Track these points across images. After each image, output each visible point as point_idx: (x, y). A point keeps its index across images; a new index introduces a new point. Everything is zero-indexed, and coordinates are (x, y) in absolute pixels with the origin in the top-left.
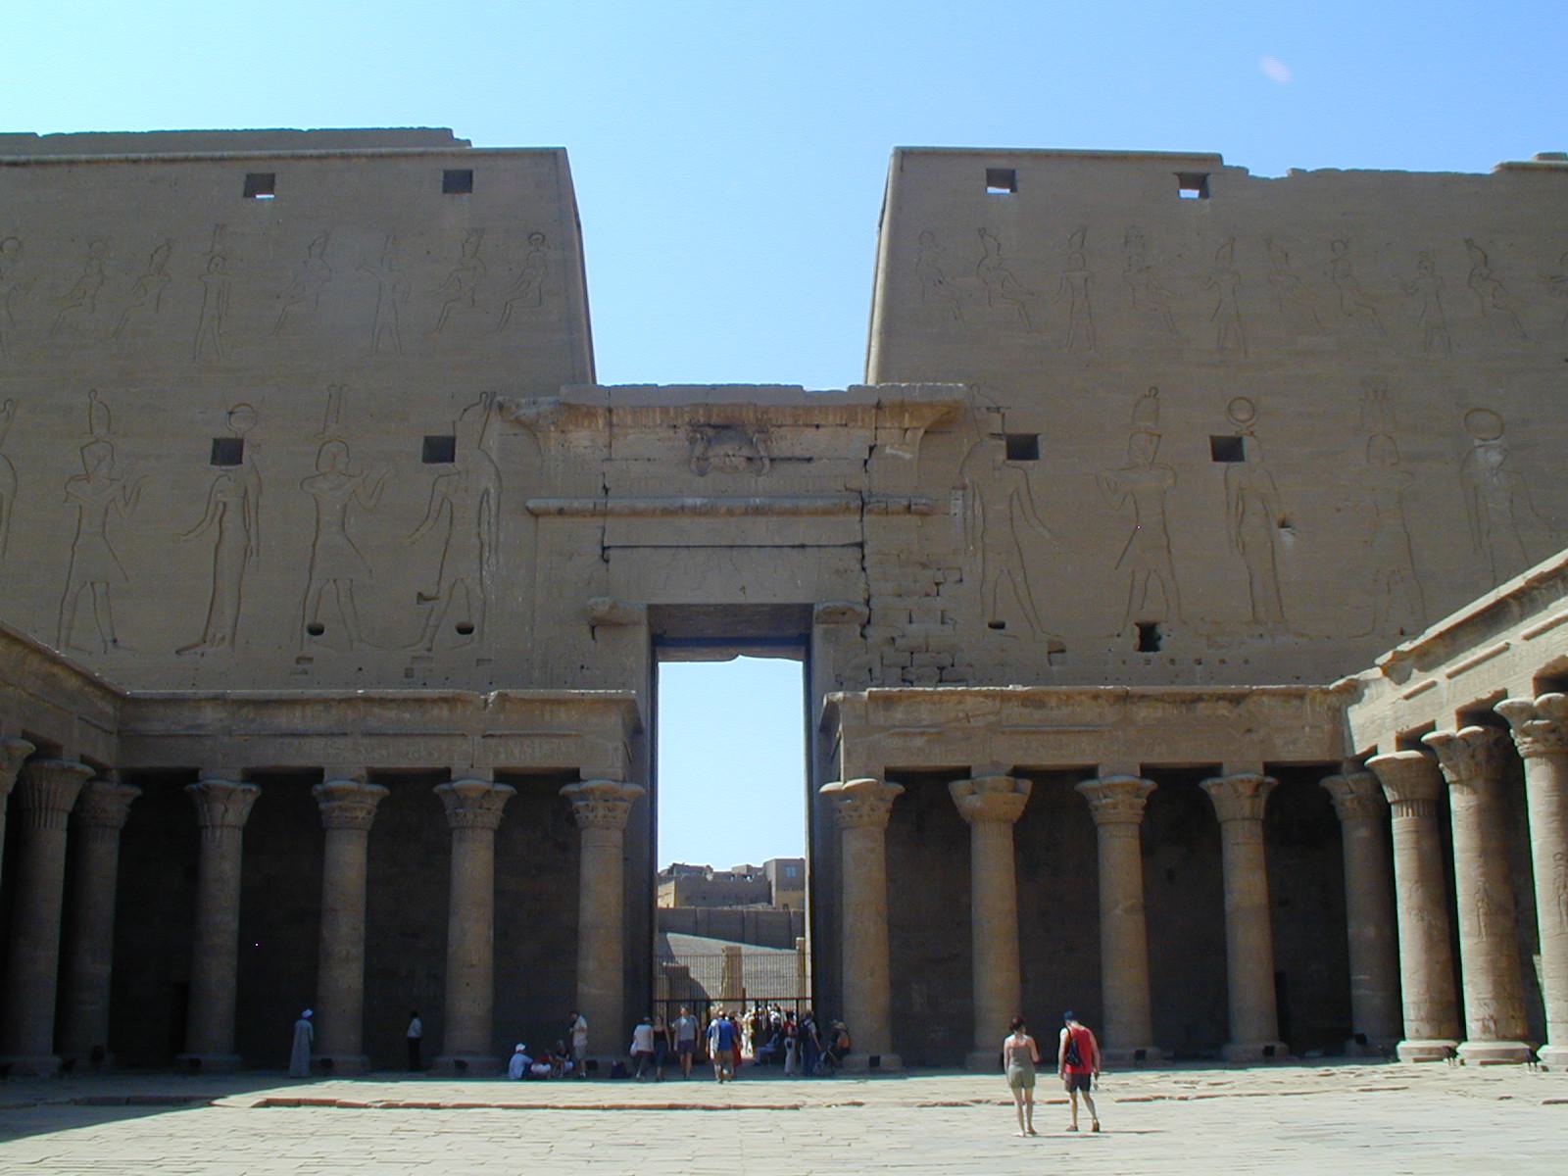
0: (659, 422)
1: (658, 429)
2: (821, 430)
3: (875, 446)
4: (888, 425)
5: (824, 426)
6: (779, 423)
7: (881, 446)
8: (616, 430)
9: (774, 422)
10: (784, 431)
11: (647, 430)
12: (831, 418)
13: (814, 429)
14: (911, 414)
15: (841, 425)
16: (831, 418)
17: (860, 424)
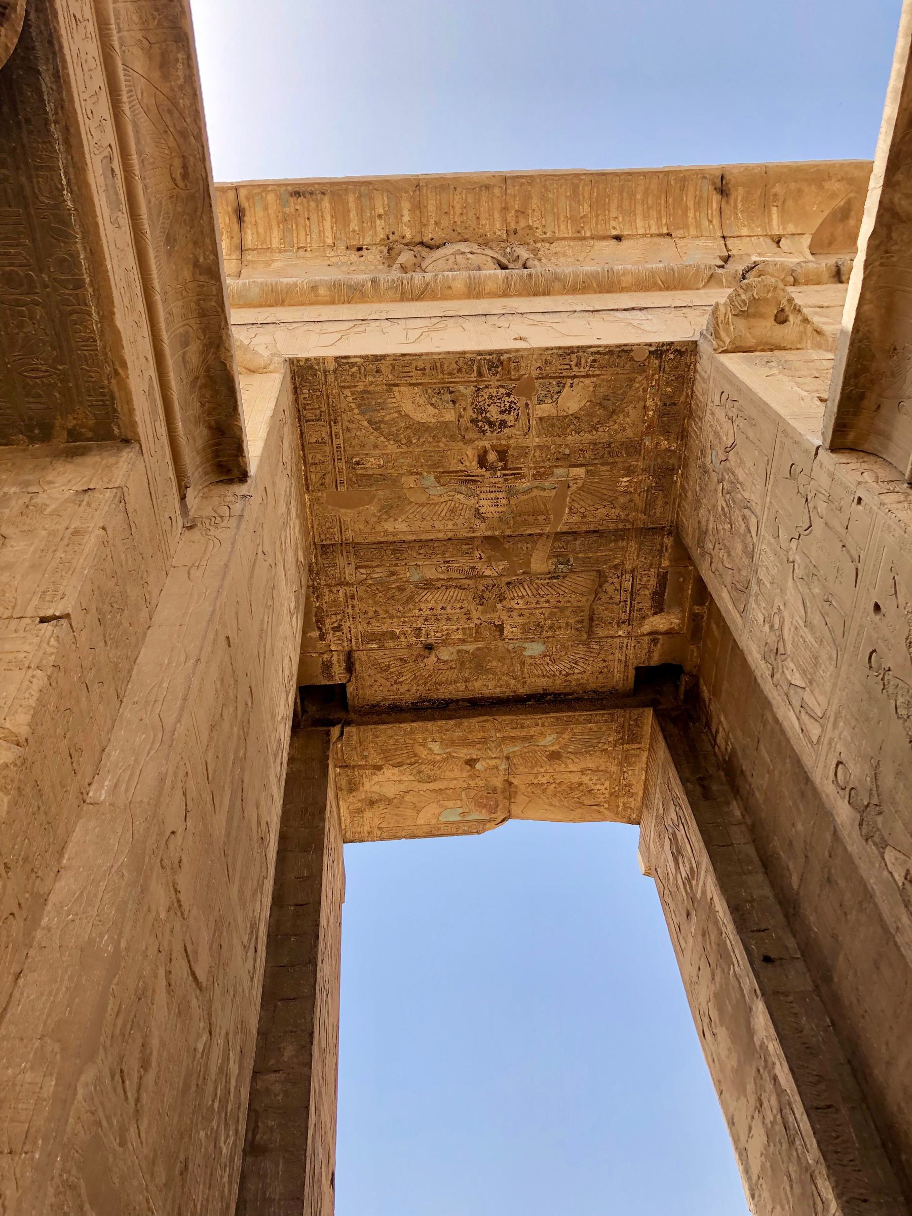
0: (329, 241)
1: (330, 253)
2: (625, 243)
3: (729, 256)
4: (745, 232)
5: (630, 237)
6: (549, 235)
7: (740, 255)
8: (250, 256)
9: (539, 234)
10: (557, 247)
11: (308, 254)
12: (640, 223)
13: (614, 242)
14: (783, 211)
15: (660, 235)
16: (640, 223)
17: (693, 232)
